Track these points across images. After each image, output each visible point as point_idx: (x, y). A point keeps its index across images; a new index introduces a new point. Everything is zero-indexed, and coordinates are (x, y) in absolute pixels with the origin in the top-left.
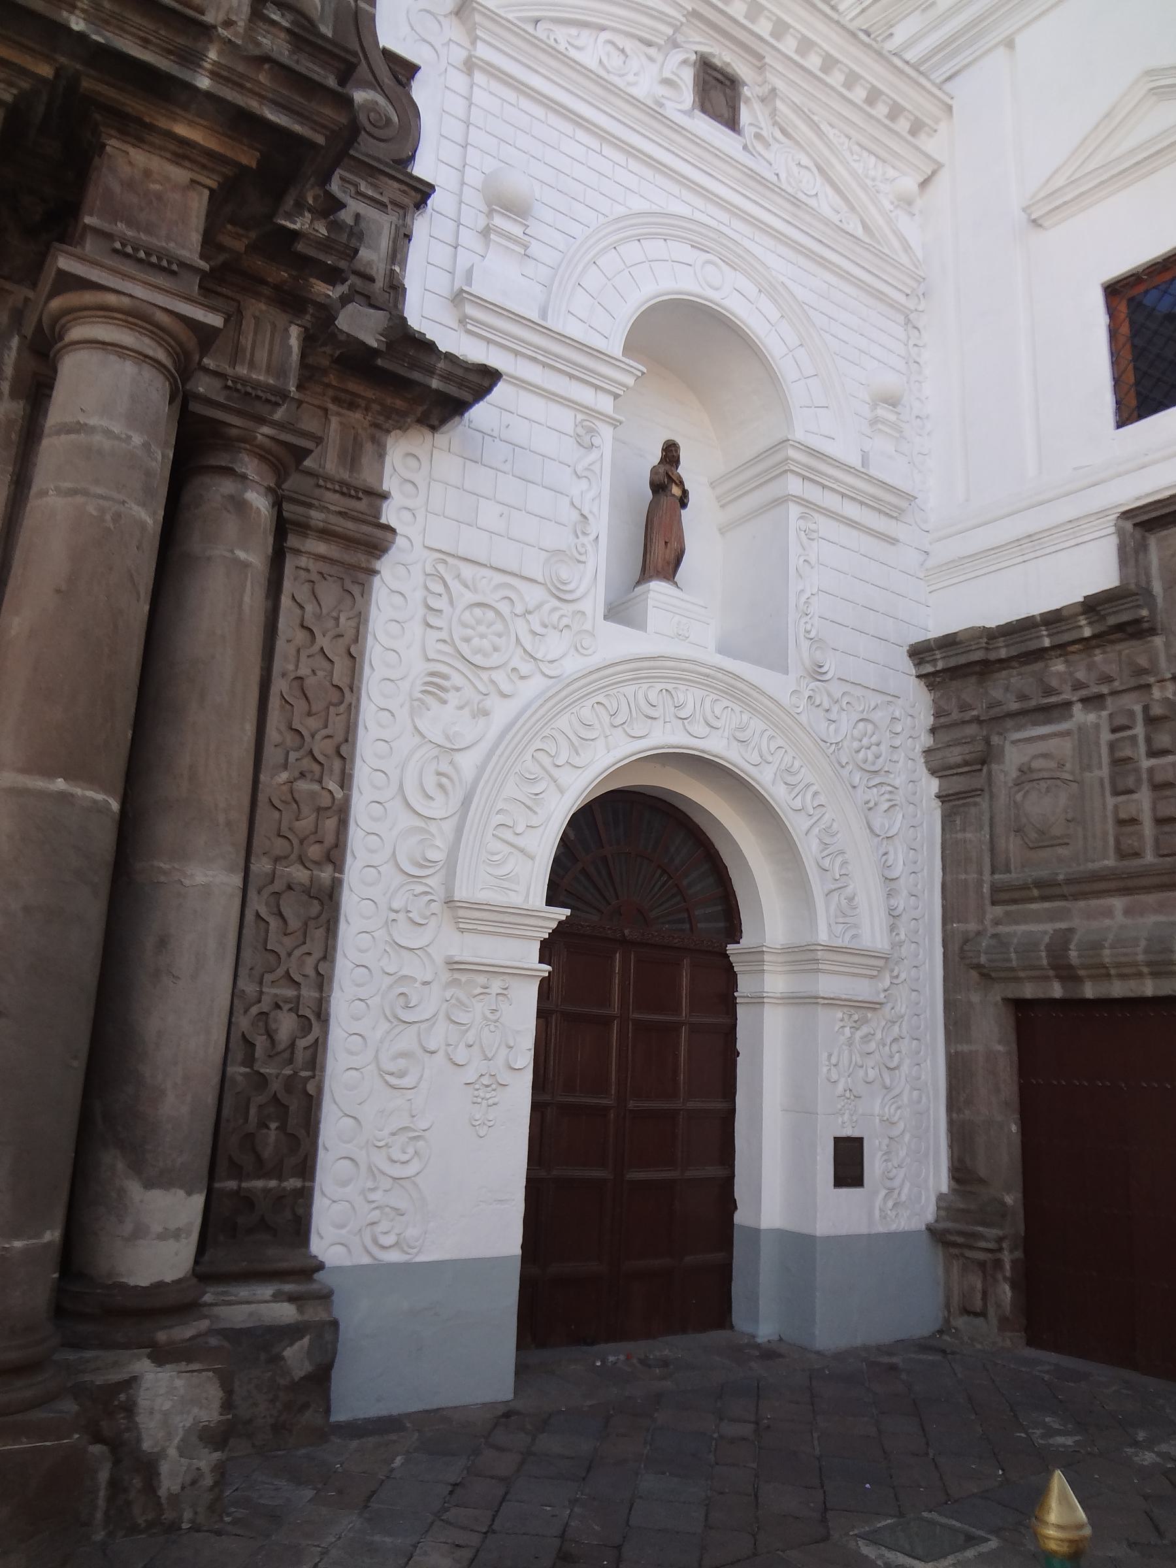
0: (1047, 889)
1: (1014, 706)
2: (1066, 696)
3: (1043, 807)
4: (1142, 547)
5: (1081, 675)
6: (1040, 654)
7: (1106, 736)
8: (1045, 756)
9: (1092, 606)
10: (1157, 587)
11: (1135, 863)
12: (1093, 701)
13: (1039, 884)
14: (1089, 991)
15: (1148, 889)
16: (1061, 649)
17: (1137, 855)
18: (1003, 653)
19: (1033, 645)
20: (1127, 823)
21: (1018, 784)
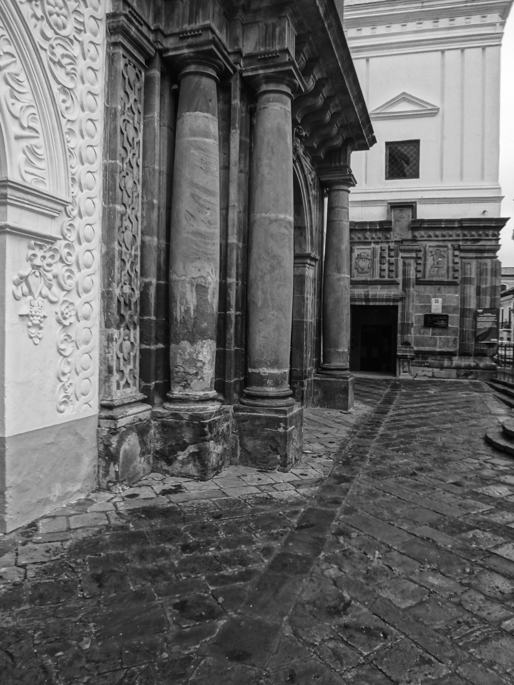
0: (365, 283)
1: (357, 240)
2: (370, 240)
3: (363, 264)
4: (391, 211)
5: (374, 236)
6: (365, 230)
7: (379, 251)
8: (365, 253)
9: (381, 223)
10: (393, 221)
11: (382, 279)
12: (377, 243)
13: (363, 281)
14: (371, 304)
15: (386, 284)
16: (370, 230)
17: (384, 277)
18: (357, 228)
19: (365, 228)
20: (382, 270)
21: (357, 258)
